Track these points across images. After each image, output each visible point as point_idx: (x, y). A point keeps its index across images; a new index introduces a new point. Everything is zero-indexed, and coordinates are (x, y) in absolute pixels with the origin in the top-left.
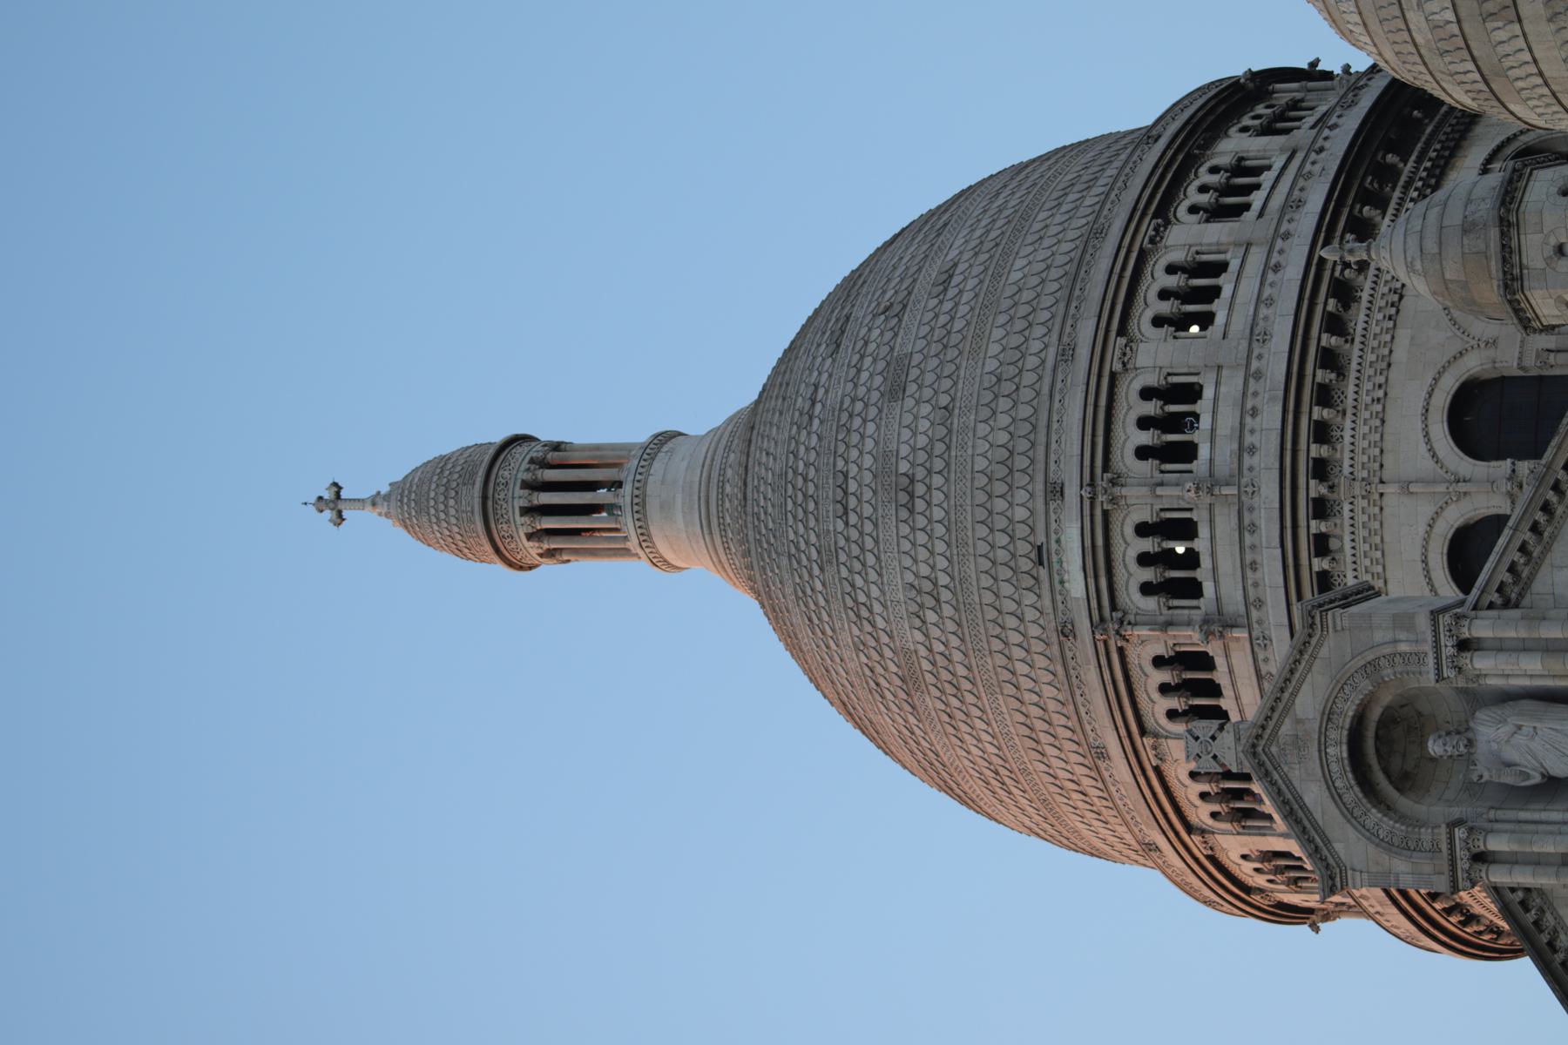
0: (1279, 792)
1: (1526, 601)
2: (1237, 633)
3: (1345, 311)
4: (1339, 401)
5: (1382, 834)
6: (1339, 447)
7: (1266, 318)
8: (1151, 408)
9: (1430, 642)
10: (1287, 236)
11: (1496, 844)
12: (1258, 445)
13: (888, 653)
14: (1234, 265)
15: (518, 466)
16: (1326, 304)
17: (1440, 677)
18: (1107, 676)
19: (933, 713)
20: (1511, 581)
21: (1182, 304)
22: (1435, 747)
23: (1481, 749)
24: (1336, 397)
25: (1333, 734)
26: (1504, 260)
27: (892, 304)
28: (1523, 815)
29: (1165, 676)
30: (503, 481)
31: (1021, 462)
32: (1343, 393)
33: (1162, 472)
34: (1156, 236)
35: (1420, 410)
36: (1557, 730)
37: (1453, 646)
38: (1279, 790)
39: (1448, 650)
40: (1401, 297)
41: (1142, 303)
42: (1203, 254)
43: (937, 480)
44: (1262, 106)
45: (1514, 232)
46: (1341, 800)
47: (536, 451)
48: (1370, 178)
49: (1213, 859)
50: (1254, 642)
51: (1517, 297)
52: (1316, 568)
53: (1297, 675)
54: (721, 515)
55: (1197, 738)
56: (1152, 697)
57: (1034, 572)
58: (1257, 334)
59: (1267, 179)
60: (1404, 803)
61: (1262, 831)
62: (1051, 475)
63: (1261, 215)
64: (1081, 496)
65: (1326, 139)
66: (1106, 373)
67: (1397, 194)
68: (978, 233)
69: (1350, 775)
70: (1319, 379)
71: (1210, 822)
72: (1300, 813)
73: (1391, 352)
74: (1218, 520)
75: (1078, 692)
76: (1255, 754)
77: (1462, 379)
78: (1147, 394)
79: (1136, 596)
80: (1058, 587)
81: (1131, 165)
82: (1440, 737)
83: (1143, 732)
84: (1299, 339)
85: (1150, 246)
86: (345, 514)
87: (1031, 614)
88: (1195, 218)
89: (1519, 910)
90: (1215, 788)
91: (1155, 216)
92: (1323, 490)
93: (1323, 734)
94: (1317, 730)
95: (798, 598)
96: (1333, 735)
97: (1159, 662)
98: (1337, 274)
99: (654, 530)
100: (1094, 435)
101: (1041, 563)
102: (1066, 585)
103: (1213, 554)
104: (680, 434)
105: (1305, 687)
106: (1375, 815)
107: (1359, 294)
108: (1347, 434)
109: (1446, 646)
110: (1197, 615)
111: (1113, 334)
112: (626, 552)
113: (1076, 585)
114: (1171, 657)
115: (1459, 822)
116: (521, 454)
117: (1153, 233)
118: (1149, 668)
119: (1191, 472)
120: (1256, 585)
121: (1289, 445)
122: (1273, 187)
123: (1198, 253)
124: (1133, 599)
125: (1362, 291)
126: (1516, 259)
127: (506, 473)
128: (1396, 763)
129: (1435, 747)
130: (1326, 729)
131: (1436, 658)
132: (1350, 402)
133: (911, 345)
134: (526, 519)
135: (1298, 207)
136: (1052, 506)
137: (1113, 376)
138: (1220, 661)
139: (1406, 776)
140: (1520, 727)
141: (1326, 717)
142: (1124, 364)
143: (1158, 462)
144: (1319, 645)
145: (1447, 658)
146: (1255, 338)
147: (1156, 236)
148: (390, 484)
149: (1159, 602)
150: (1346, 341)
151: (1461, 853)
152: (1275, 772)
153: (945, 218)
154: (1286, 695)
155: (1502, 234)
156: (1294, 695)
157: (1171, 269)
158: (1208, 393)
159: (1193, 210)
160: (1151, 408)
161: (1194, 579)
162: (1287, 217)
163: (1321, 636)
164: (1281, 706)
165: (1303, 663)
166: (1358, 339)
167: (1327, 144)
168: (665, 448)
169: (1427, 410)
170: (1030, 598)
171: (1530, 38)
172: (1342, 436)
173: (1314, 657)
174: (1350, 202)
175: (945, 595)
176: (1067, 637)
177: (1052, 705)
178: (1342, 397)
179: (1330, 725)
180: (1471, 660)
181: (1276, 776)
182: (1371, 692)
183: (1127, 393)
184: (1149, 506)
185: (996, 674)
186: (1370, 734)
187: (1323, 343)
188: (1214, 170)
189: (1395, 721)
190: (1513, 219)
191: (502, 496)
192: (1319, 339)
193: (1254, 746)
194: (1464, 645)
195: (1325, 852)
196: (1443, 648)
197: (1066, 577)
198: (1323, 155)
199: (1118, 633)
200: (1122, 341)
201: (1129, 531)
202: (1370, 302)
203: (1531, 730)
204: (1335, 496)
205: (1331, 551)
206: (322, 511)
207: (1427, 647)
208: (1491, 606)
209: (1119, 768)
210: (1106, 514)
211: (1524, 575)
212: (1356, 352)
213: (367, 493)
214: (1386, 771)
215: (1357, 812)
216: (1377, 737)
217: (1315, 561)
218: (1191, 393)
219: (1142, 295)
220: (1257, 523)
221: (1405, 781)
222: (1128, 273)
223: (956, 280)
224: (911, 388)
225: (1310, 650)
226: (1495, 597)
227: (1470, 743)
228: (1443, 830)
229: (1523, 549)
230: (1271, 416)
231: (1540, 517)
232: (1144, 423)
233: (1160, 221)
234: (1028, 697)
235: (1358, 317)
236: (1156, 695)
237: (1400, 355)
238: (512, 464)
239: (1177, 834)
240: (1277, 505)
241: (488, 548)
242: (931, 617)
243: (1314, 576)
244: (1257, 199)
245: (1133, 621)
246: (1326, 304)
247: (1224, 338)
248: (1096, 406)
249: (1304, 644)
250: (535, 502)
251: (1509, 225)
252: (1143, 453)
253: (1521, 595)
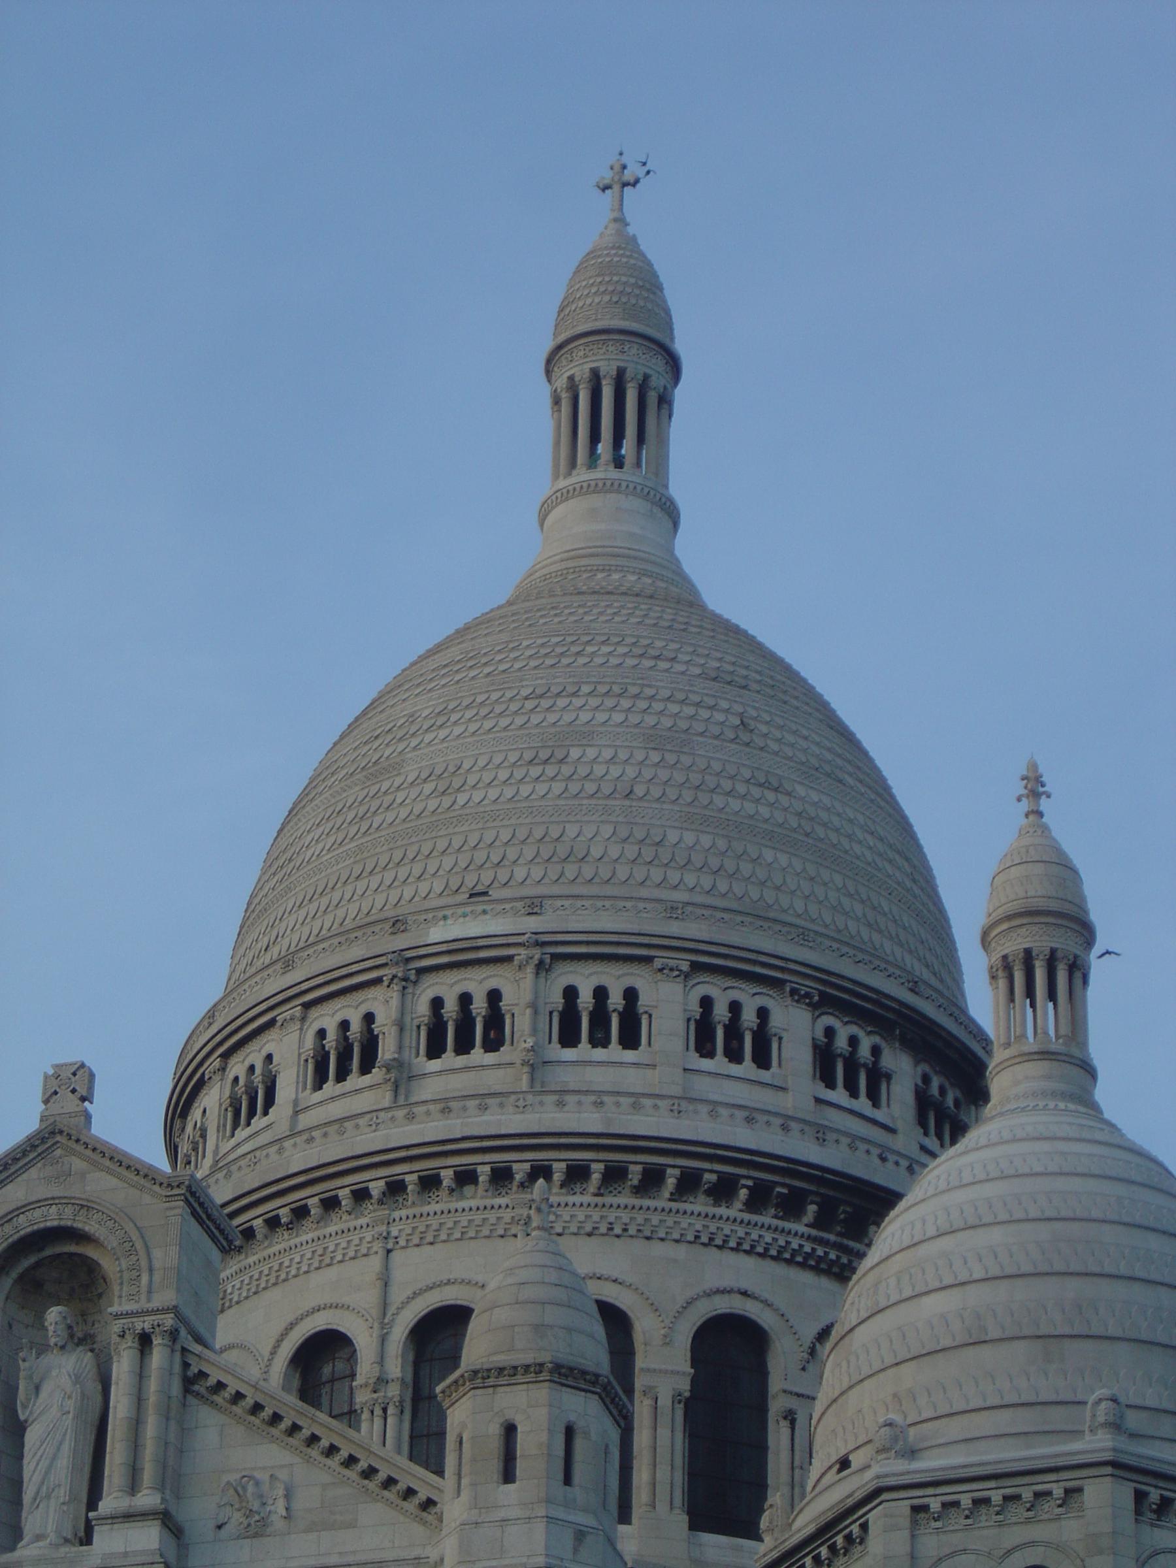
0: (15, 1160)
1: (191, 1399)
2: (389, 1096)
3: (705, 1191)
4: (611, 1189)
6: (563, 1191)
7: (696, 1112)
8: (616, 1000)
9: (147, 1306)
10: (785, 1128)
12: (566, 1108)
13: (401, 747)
14: (764, 1075)
16: (711, 1171)
18: (355, 968)
19: (344, 795)
20: (208, 1385)
21: (725, 1026)
22: (53, 1314)
24: (616, 1186)
25: (69, 1210)
26: (501, 1370)
27: (751, 731)
29: (356, 1027)
30: (626, 349)
31: (570, 871)
32: (620, 1192)
33: (551, 1013)
34: (799, 995)
35: (599, 1272)
36: (65, 1434)
37: (143, 1329)
38: (18, 1159)
40: (719, 1247)
41: (726, 985)
42: (780, 1044)
43: (558, 788)
44: (959, 1094)
45: (530, 1377)
46: (7, 1222)
48: (848, 1209)
50: (374, 1114)
51: (468, 1384)
52: (443, 1173)
53: (125, 1173)
54: (577, 569)
55: (74, 1074)
56: (338, 1014)
57: (463, 889)
58: (684, 1102)
59: (863, 1104)
61: (221, 1128)
62: (550, 902)
63: (818, 1101)
64: (524, 934)
65: (897, 1163)
66: (652, 953)
67: (832, 1237)
68: (824, 815)
69: (29, 1230)
70: (632, 1168)
71: (231, 1076)
73: (662, 1239)
74: (500, 1072)
75: (342, 939)
76: (53, 1133)
77: (630, 1313)
78: (631, 995)
79: (430, 994)
80: (440, 914)
81: (883, 966)
82: (65, 1318)
83: (307, 1006)
84: (674, 1146)
85: (788, 989)
86: (608, 192)
87: (424, 887)
88: (820, 1034)
90: (257, 1080)
91: (822, 994)
92: (446, 1183)
94: (73, 1195)
95: (467, 652)
97: (369, 1018)
98: (743, 1182)
99: (572, 503)
100: (588, 943)
101: (471, 896)
102: (442, 923)
103: (467, 1068)
104: (676, 524)
105: (114, 1182)
107: (724, 1204)
108: (577, 1199)
109: (144, 1322)
110: (406, 1054)
111: (694, 958)
112: (556, 476)
113: (437, 933)
114: (373, 1030)
116: (656, 366)
117: (803, 992)
118: (363, 1009)
119: (550, 1042)
120: (428, 1113)
121: (563, 1140)
122: (851, 1112)
123: (780, 1039)
124: (430, 988)
125: (728, 1207)
127: (634, 351)
130: (73, 1204)
131: (132, 1313)
132: (608, 1200)
133: (703, 753)
134: (587, 375)
135: (818, 1138)
136: (519, 905)
137: (648, 960)
138: (367, 1079)
139: (38, 1285)
141: (85, 1203)
142: (661, 970)
143: (560, 1009)
145: (133, 1323)
146: (676, 1101)
147: (799, 995)
148: (634, 235)
149: (424, 1016)
150: (672, 1194)
152: (36, 1154)
153: (850, 781)
154: (108, 1163)
156: (109, 1171)
157: (763, 1013)
158: (629, 1055)
159: (830, 1032)
160: (616, 1000)
161: (444, 1051)
162: (807, 1128)
163: (161, 1195)
165: (136, 1178)
166: (674, 1205)
167: (890, 1165)
168: (656, 510)
169: (599, 1278)
170: (438, 887)
171: (881, 1375)
172: (575, 1194)
173: (142, 1189)
174: (822, 1191)
175: (447, 801)
176: (394, 925)
177: (341, 913)
178: (615, 1192)
179: (77, 1208)
180: (130, 1347)
181: (32, 1156)
182: (105, 1248)
183: (632, 974)
184: (516, 1002)
185: (372, 856)
186: (72, 1248)
187: (669, 1171)
188: (876, 1051)
191: (611, 348)
192: (674, 1166)
193: (61, 1132)
196: (142, 1319)
197: (449, 922)
198: (877, 1161)
199: (394, 977)
200: (685, 967)
201: (493, 984)
202: (714, 1216)
203: (67, 1409)
204: (515, 1188)
205: (462, 1187)
206: (612, 168)
207: (143, 1304)
209: (275, 984)
210: (509, 959)
211: (215, 1397)
212: (660, 1204)
214: (37, 1265)
216: (71, 1255)
217: (450, 1172)
218: (630, 1039)
219: (735, 985)
220: (488, 1112)
222: (759, 970)
223: (771, 796)
224: (655, 757)
225: (148, 1184)
226: (194, 1369)
230: (590, 1121)
232: (601, 994)
233: (816, 998)
234: (349, 889)
235: (699, 1204)
236: (339, 1018)
237: (657, 1249)
238: (644, 356)
239: (221, 1043)
240: (503, 1132)
241: (562, 338)
242: (428, 788)
243: (401, 1177)
244: (839, 1095)
245: (407, 991)
246: (711, 1171)
247: (685, 1070)
248: (618, 944)
249: (153, 1179)
250: (604, 382)
252: (571, 993)
253: (197, 1395)
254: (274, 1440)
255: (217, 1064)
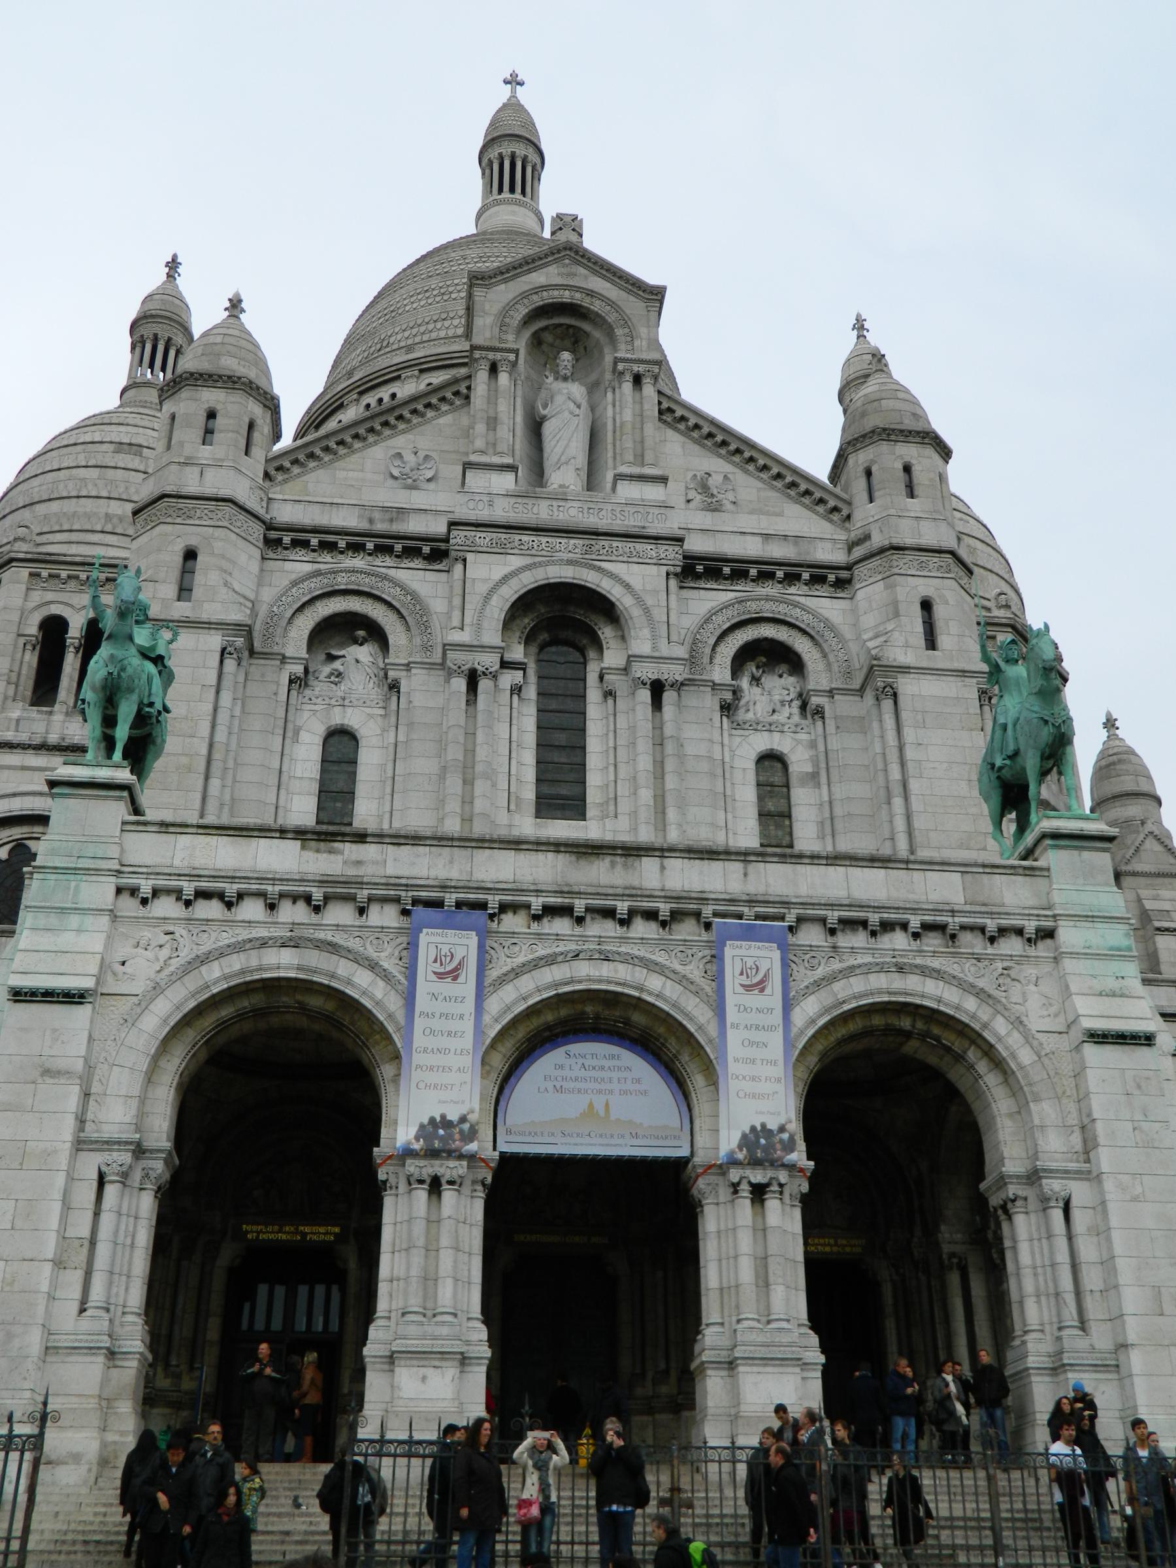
5: (511, 313)
11: (503, 378)
15: (533, 157)
17: (616, 361)
23: (561, 385)
28: (519, 401)
39: (636, 368)
45: (918, 440)
47: (539, 167)
49: (341, 406)
60: (527, 334)
72: (525, 268)
76: (565, 249)
86: (509, 86)
89: (455, 388)
93: (578, 289)
96: (578, 295)
105: (608, 285)
106: (523, 311)
115: (517, 357)
126: (902, 439)
128: (548, 337)
129: (566, 356)
140: (579, 407)
144: (637, 296)
151: (498, 356)
155: (918, 433)
156: (604, 277)
164: (597, 268)
173: (629, 292)
189: (576, 342)
190: (926, 441)
194: (637, 380)
195: (499, 278)
208: (660, 403)
213: (519, 95)
214: (545, 328)
215: (525, 301)
216: (569, 326)
221: (537, 341)
226: (665, 405)
227: (565, 379)
228: (515, 346)
229: (697, 427)
231: (719, 438)
251: (924, 438)
253: (665, 422)
254: (720, 456)
255: (355, 396)
